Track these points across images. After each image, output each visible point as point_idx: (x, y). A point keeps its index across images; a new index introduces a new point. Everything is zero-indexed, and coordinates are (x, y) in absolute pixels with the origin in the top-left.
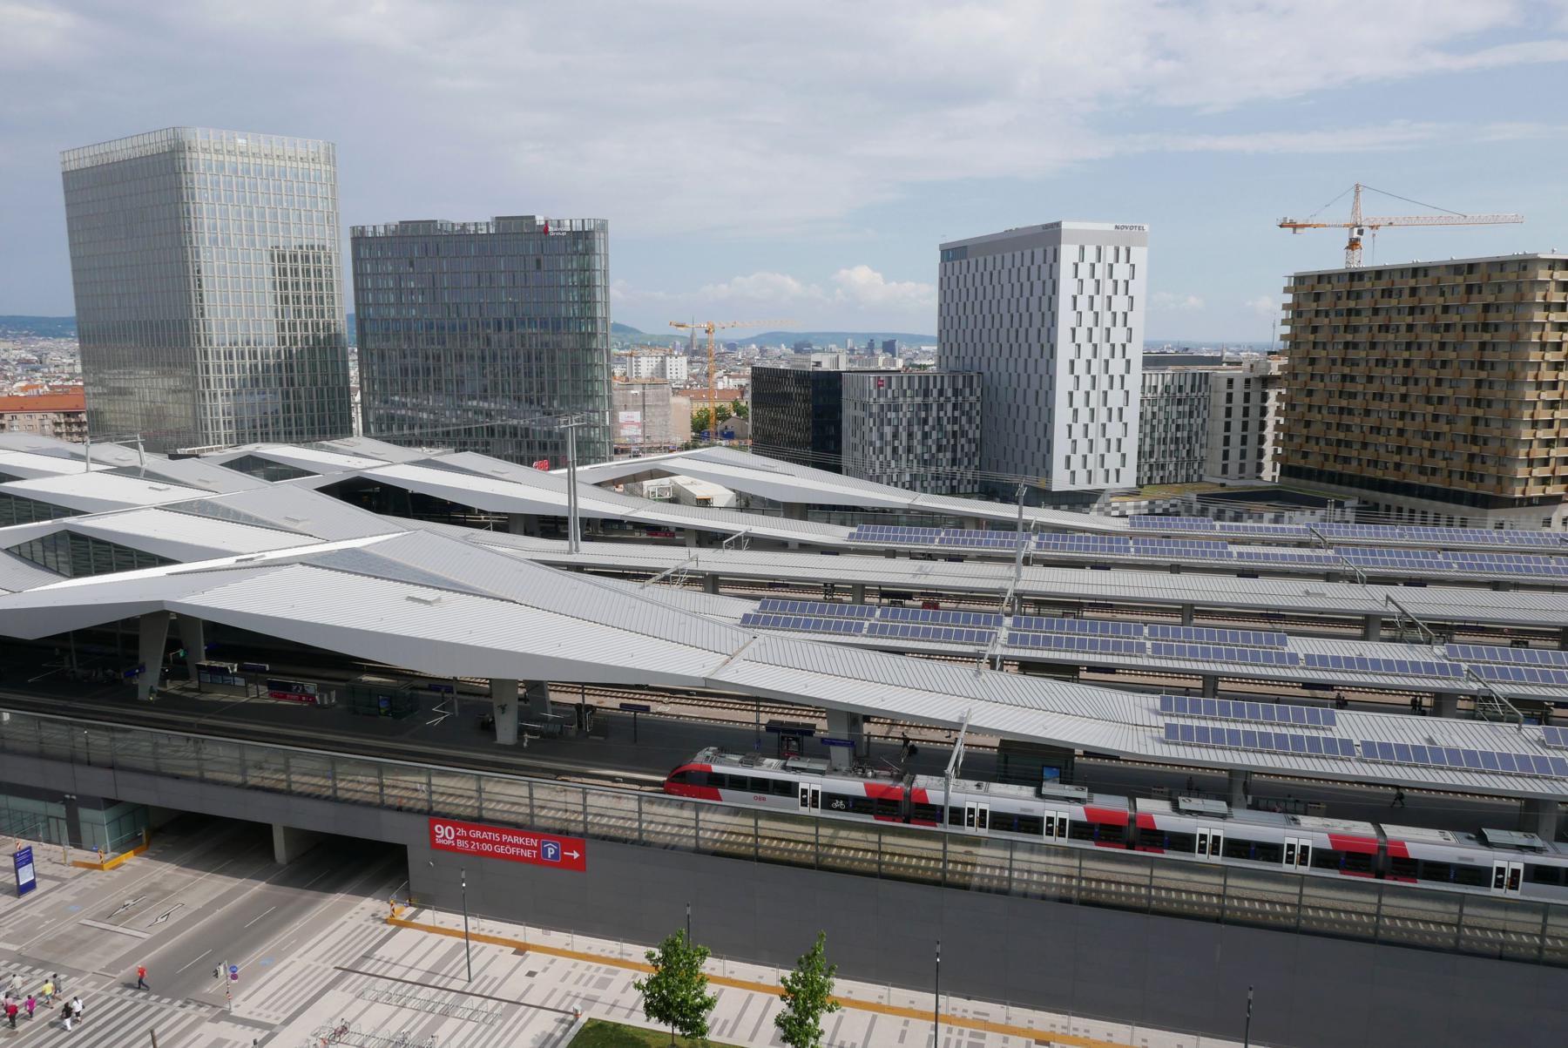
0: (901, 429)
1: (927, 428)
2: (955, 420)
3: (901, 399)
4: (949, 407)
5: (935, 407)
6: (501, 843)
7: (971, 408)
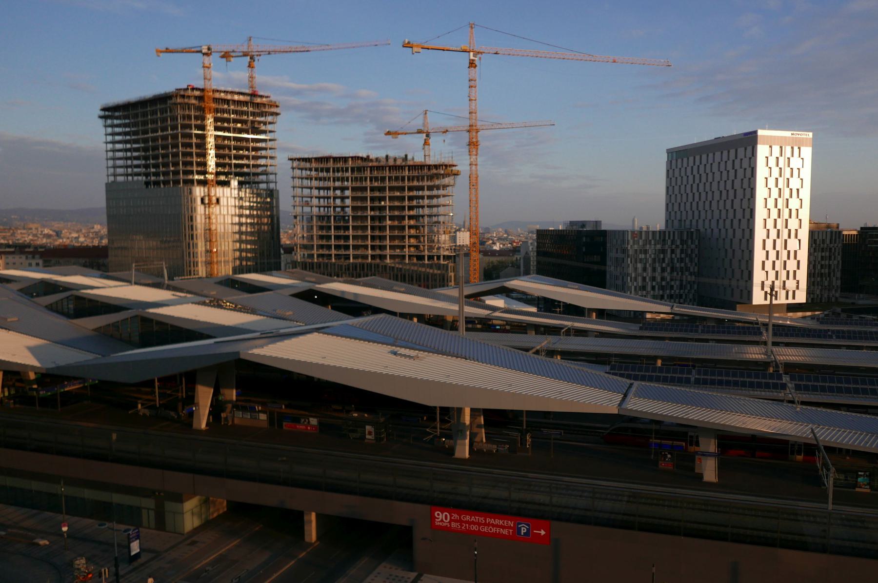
0: (648, 265)
1: (664, 265)
2: (681, 260)
3: (648, 246)
4: (678, 251)
5: (669, 251)
6: (485, 524)
7: (692, 252)
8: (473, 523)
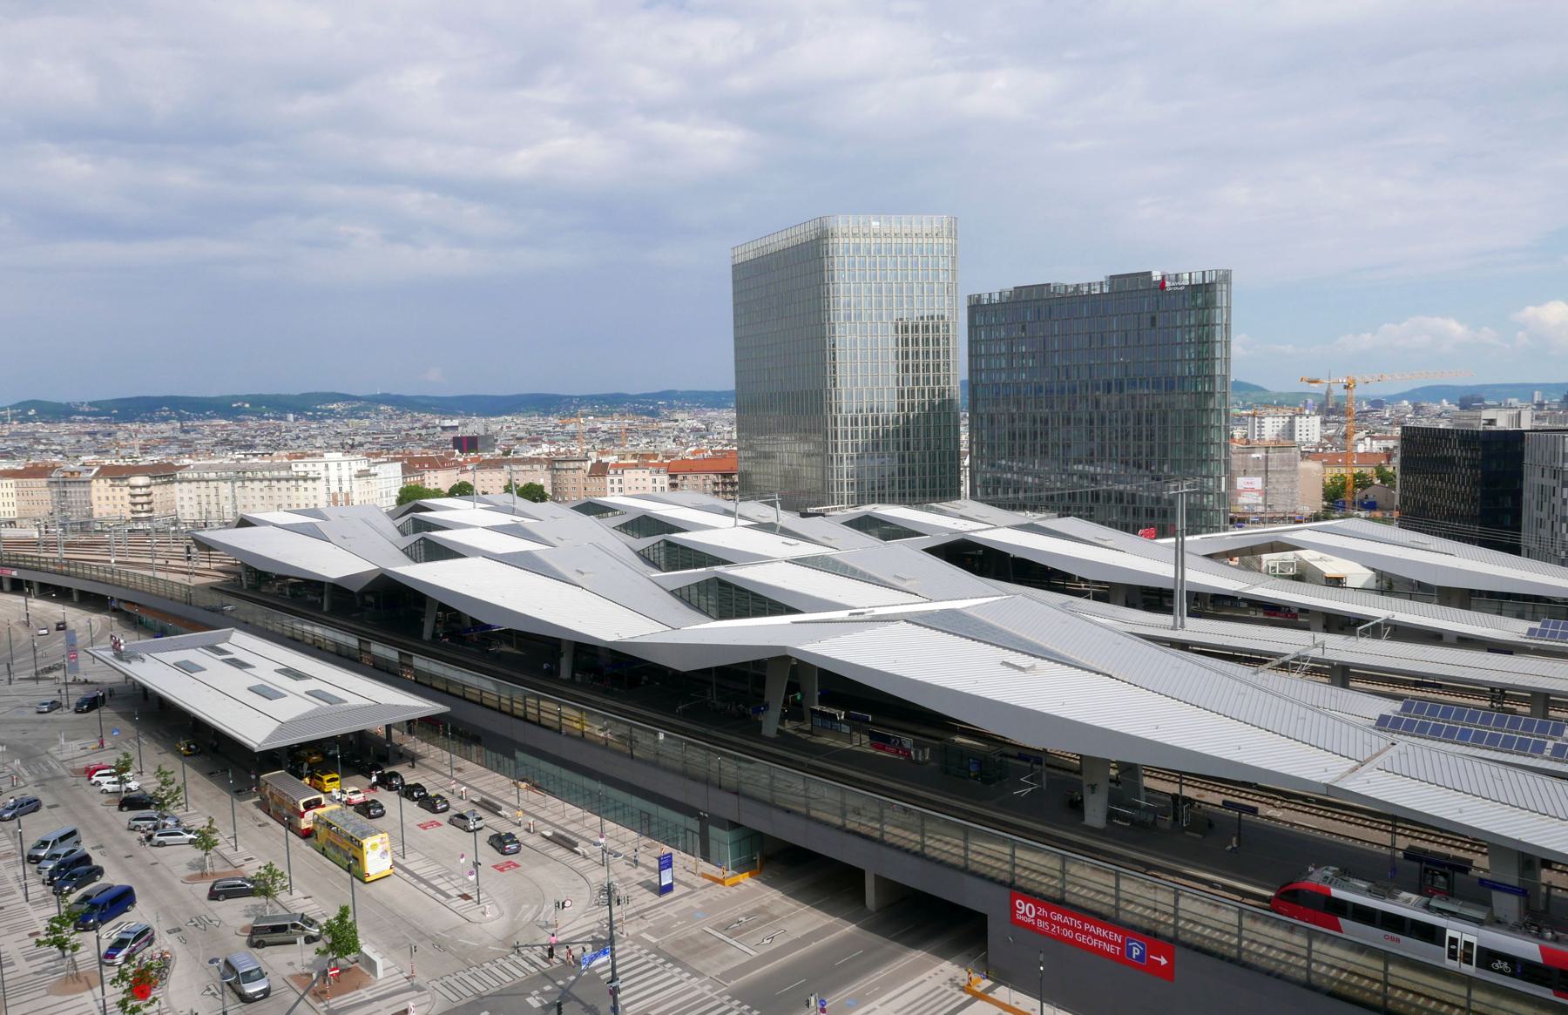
6: (1082, 932)
8: (1068, 927)
